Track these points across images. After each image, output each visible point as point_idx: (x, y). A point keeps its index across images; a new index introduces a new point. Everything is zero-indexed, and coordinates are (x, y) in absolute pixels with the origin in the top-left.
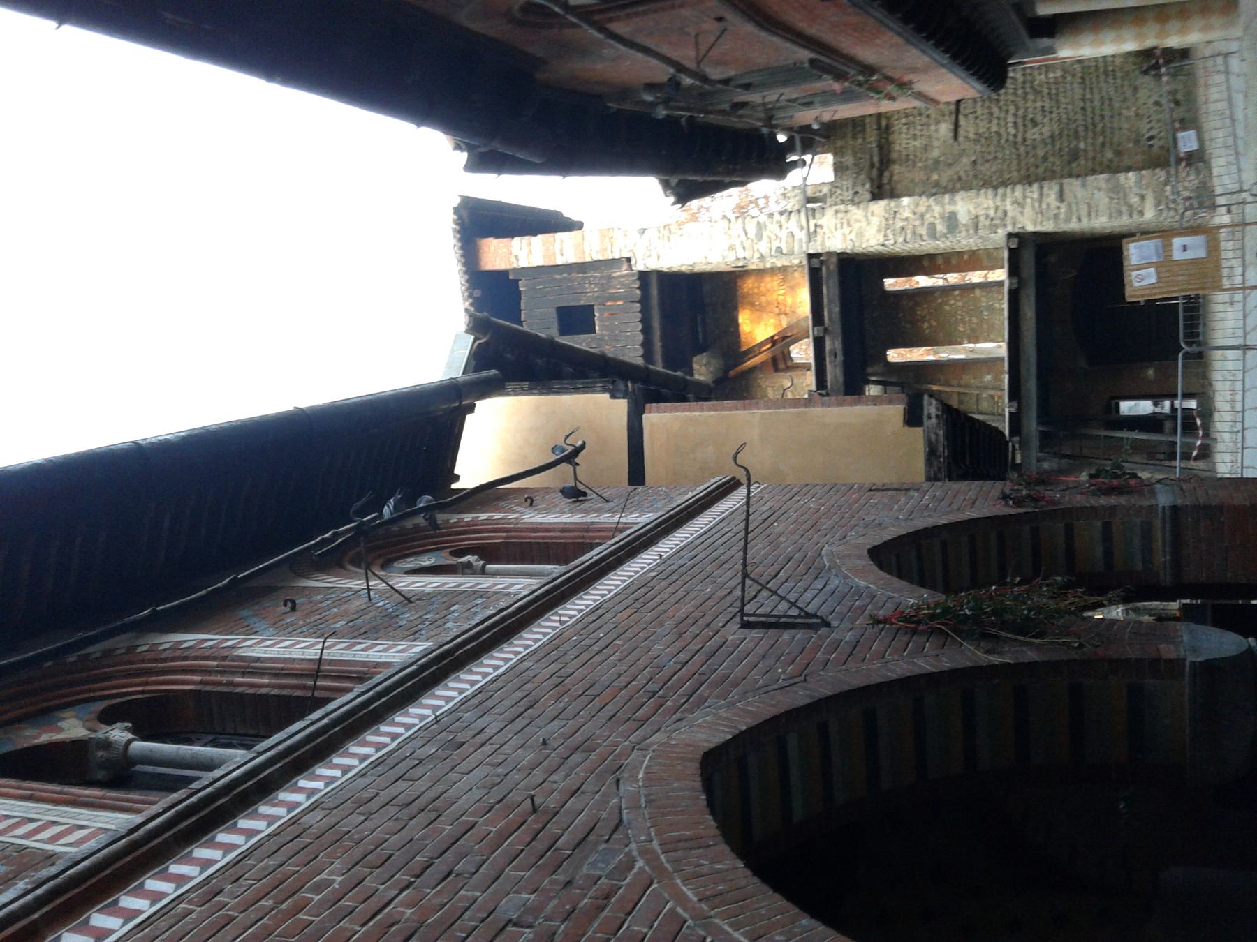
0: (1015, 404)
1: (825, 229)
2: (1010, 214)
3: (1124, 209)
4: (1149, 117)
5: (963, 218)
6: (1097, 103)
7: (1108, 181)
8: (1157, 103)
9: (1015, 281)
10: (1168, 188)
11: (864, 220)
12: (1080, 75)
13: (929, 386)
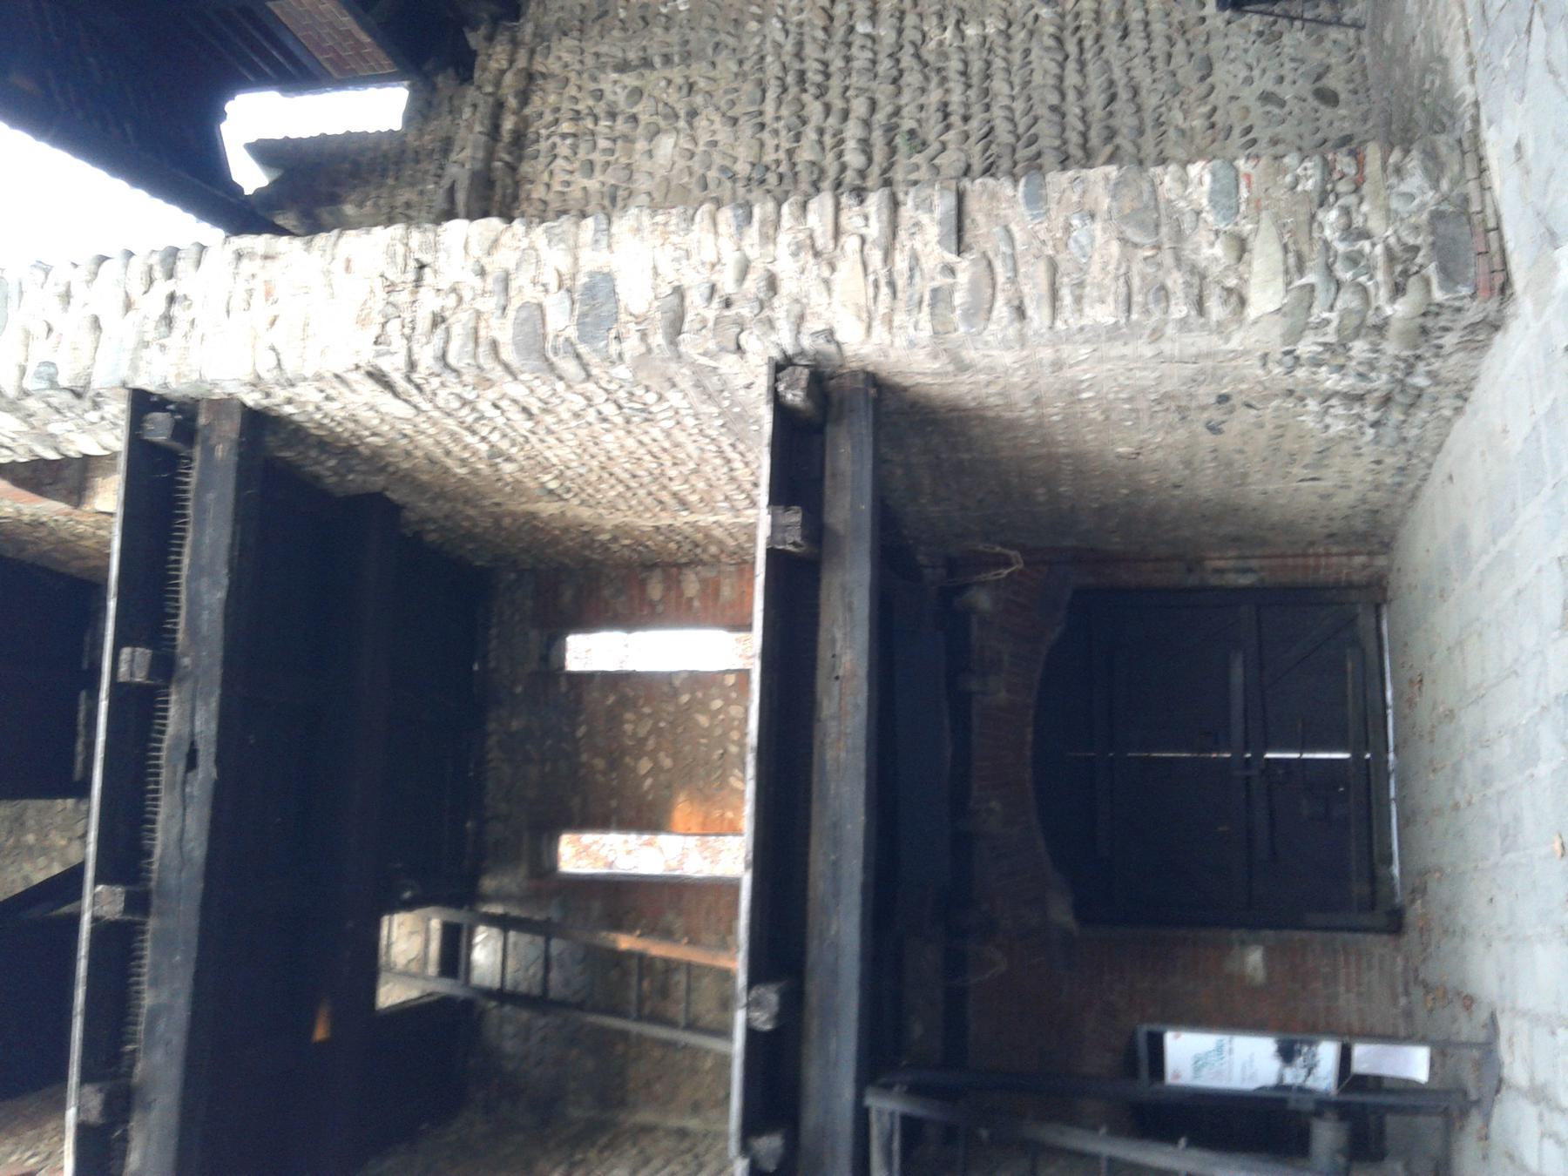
0: (771, 995)
2: (787, 287)
3: (1176, 281)
4: (1249, 130)
6: (1096, 98)
7: (1116, 189)
8: (1266, 97)
9: (794, 517)
10: (1331, 216)
12: (1051, 30)
13: (613, 936)
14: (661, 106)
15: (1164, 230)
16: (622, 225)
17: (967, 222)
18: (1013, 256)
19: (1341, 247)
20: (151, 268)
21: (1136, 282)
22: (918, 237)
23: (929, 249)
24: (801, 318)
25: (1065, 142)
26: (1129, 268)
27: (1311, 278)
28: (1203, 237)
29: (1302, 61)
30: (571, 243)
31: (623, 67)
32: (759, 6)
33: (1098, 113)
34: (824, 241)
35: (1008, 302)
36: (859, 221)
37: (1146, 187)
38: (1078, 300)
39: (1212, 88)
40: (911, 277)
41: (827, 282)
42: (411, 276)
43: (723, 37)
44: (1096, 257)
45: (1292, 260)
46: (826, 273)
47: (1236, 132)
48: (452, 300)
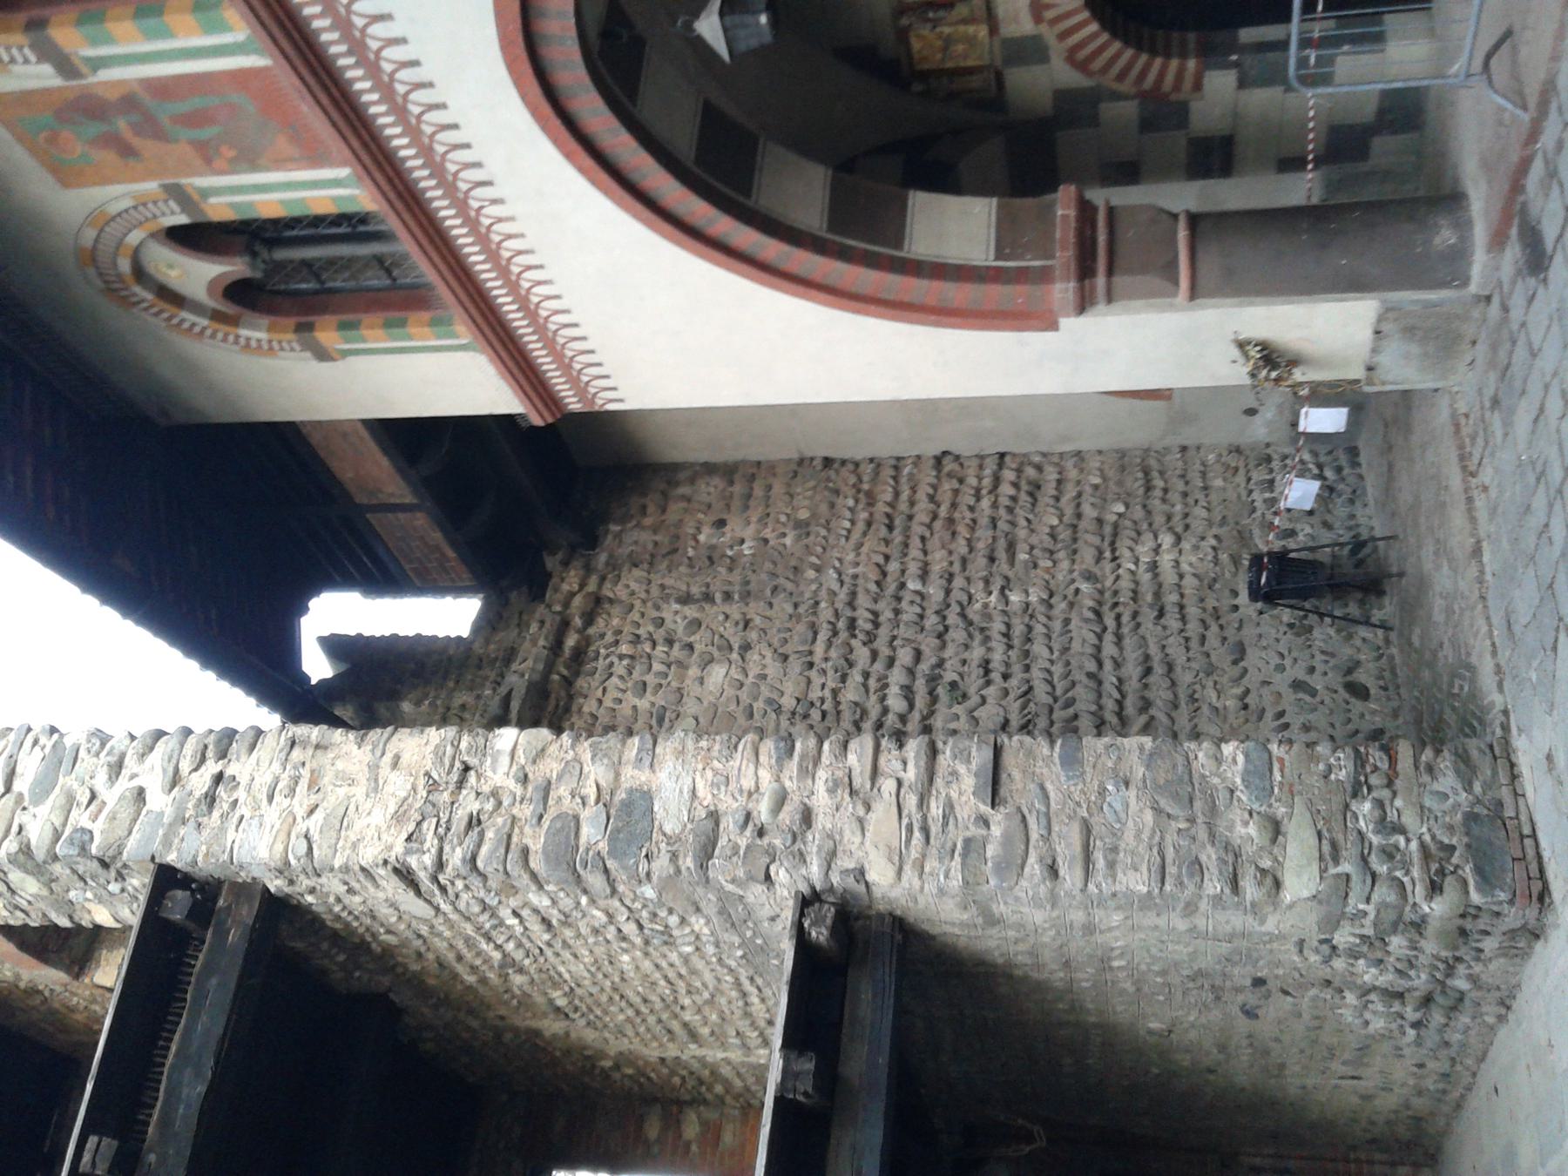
1: (241, 794)
2: (822, 821)
3: (1209, 856)
4: (1281, 714)
5: (671, 814)
6: (1132, 671)
7: (1150, 760)
8: (1297, 685)
9: (808, 1065)
11: (363, 776)
14: (716, 637)
15: (1198, 804)
16: (666, 748)
17: (1004, 776)
18: (1047, 815)
19: (1376, 840)
20: (206, 747)
21: (1170, 854)
22: (954, 786)
23: (964, 799)
24: (833, 854)
25: (1101, 708)
26: (1162, 838)
27: (1345, 867)
28: (1237, 815)
29: (1333, 655)
30: (616, 759)
31: (686, 599)
32: (818, 557)
33: (1133, 685)
34: (861, 780)
35: (1041, 860)
36: (898, 765)
37: (1180, 760)
38: (1111, 865)
39: (1245, 671)
40: (945, 824)
41: (861, 822)
42: (455, 777)
43: (782, 581)
44: (1130, 824)
45: (1326, 848)
46: (861, 811)
47: (1269, 715)
48: (489, 806)
